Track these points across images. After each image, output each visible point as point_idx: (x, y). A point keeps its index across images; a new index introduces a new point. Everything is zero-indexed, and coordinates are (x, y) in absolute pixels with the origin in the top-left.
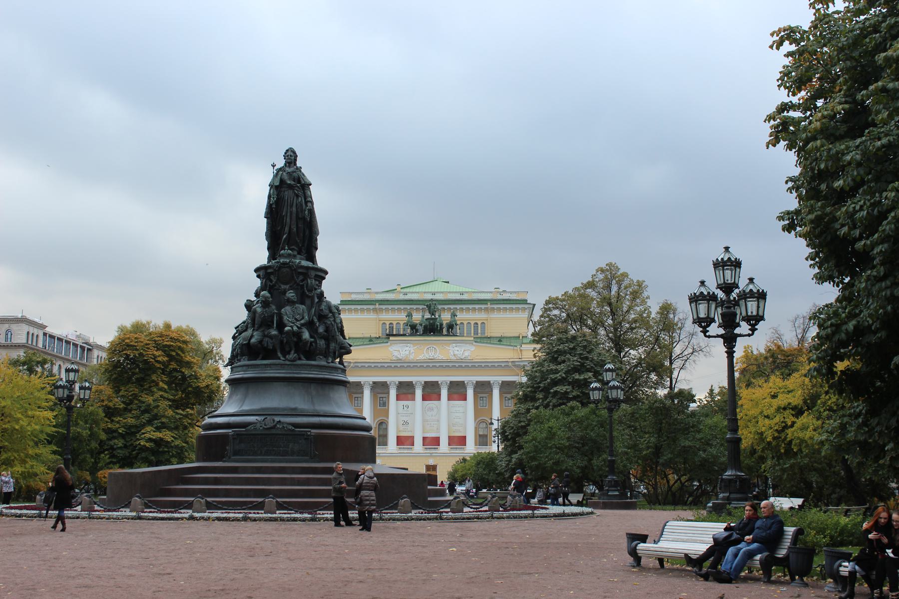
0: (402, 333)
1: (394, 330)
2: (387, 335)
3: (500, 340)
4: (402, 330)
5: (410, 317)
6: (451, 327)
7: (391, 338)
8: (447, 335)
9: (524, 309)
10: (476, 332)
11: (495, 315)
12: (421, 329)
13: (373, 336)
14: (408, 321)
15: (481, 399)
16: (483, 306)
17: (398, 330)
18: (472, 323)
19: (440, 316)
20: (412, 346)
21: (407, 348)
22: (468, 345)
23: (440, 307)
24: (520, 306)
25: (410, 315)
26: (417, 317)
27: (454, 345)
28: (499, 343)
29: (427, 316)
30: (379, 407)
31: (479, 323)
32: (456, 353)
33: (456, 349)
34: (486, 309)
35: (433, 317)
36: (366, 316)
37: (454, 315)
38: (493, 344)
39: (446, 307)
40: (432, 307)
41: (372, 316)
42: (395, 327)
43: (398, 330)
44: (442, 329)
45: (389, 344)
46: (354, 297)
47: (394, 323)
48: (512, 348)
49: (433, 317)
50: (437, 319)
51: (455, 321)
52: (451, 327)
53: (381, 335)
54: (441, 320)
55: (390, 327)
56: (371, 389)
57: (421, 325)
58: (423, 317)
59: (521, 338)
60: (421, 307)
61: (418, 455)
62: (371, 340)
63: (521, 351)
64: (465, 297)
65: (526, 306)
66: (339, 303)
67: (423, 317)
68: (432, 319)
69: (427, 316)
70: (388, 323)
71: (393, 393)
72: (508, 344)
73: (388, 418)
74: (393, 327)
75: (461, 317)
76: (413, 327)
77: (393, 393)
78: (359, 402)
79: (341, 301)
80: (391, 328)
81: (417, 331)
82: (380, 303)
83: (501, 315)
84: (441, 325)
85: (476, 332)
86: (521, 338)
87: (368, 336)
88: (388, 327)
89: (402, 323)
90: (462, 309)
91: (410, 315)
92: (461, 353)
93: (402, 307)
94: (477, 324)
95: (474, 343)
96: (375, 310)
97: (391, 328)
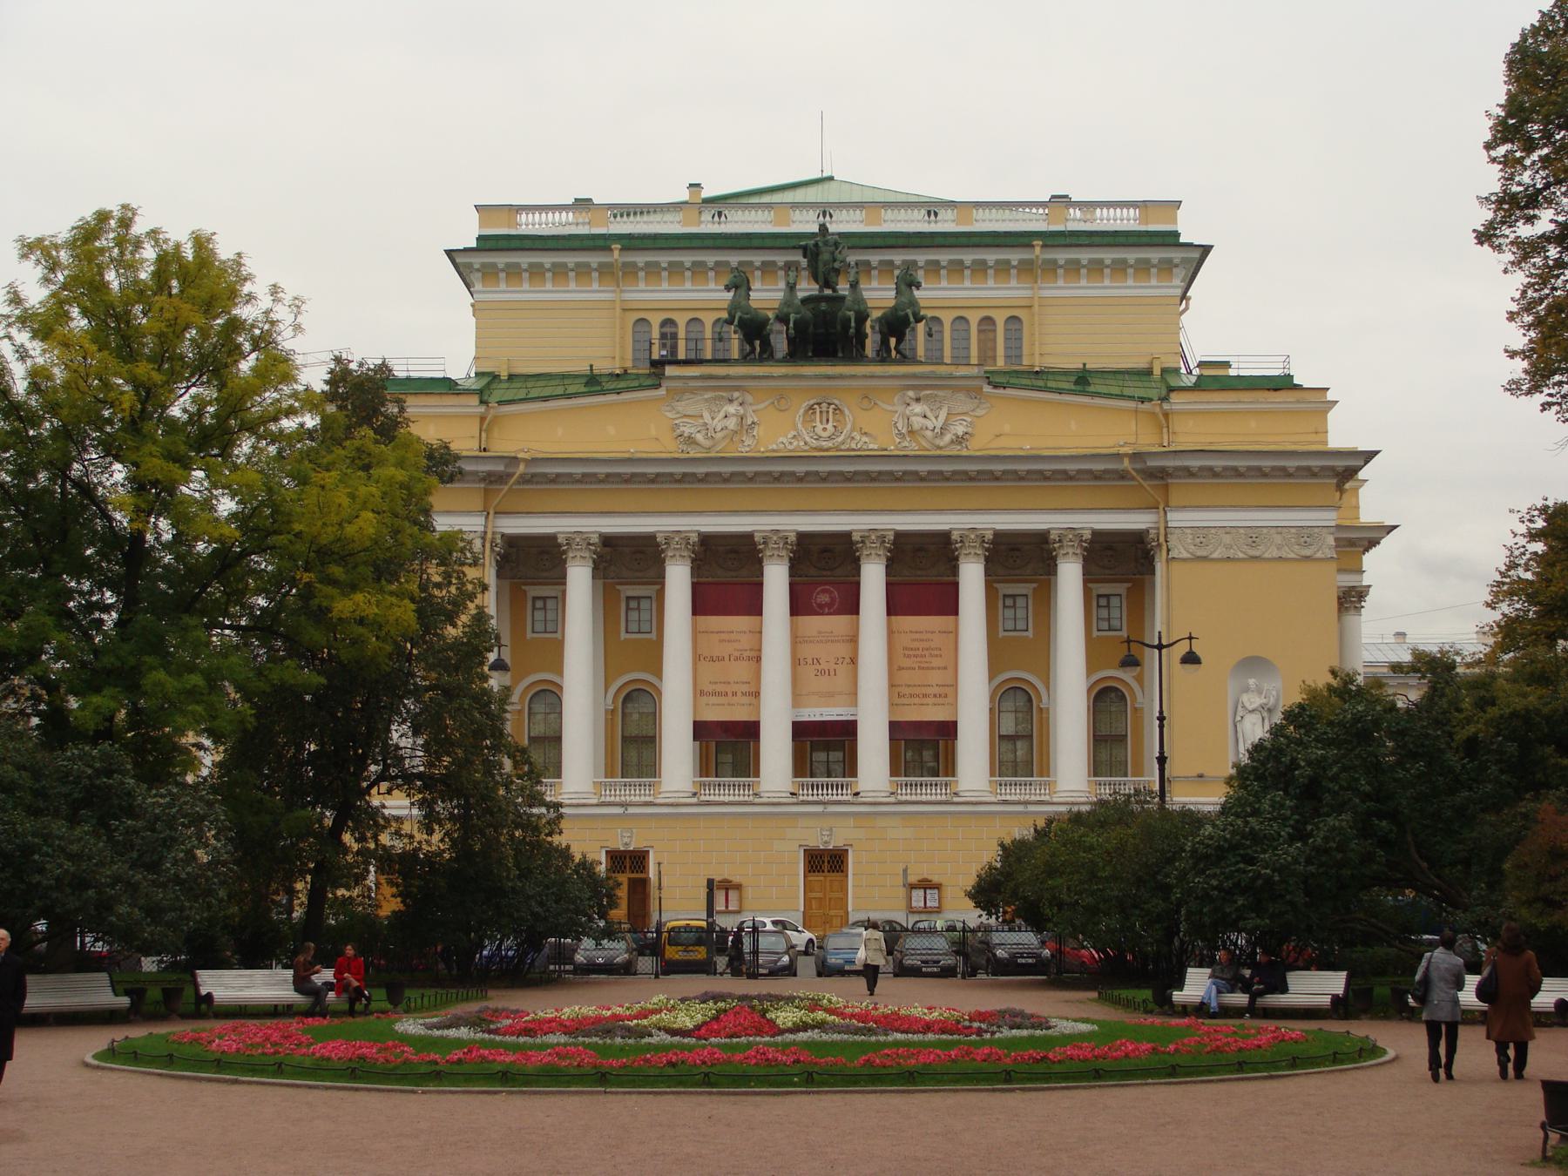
0: (709, 356)
1: (681, 345)
2: (654, 364)
3: (1082, 380)
4: (709, 343)
5: (742, 291)
6: (897, 325)
7: (670, 371)
8: (883, 357)
9: (1167, 267)
10: (987, 354)
11: (1058, 289)
12: (780, 344)
13: (603, 366)
14: (733, 308)
15: (1009, 602)
16: (1014, 256)
17: (695, 341)
18: (974, 318)
19: (854, 286)
20: (749, 398)
21: (731, 409)
22: (961, 396)
23: (852, 258)
24: (1154, 255)
25: (739, 283)
26: (766, 296)
27: (911, 393)
28: (1079, 388)
29: (807, 288)
30: (623, 636)
31: (1000, 318)
32: (917, 422)
33: (918, 408)
34: (1026, 268)
35: (828, 292)
36: (573, 292)
37: (908, 282)
38: (1060, 391)
39: (875, 258)
40: (825, 256)
41: (596, 292)
42: (682, 334)
43: (695, 341)
44: (861, 337)
45: (662, 392)
46: (529, 225)
47: (681, 320)
48: (1132, 404)
49: (828, 292)
50: (843, 298)
51: (913, 303)
52: (897, 325)
53: (629, 364)
54: (860, 301)
55: (663, 336)
56: (596, 569)
57: (782, 319)
58: (791, 288)
59: (1157, 371)
60: (781, 258)
61: (776, 815)
62: (594, 383)
63: (1166, 415)
64: (947, 223)
65: (1176, 255)
66: (474, 244)
67: (791, 288)
68: (827, 299)
69: (807, 288)
70: (656, 320)
71: (678, 579)
72: (1116, 391)
73: (660, 678)
74: (674, 336)
75: (931, 294)
76: (753, 330)
77: (678, 579)
78: (550, 616)
79: (480, 238)
80: (669, 338)
81: (767, 346)
82: (625, 242)
83: (1084, 288)
84: (862, 317)
85: (987, 354)
86: (1157, 371)
87: (583, 368)
88: (656, 334)
89: (708, 319)
90: (934, 268)
91: (739, 283)
92: (939, 423)
93: (711, 258)
94: (988, 321)
95: (987, 389)
96: (605, 271)
97: (669, 338)
